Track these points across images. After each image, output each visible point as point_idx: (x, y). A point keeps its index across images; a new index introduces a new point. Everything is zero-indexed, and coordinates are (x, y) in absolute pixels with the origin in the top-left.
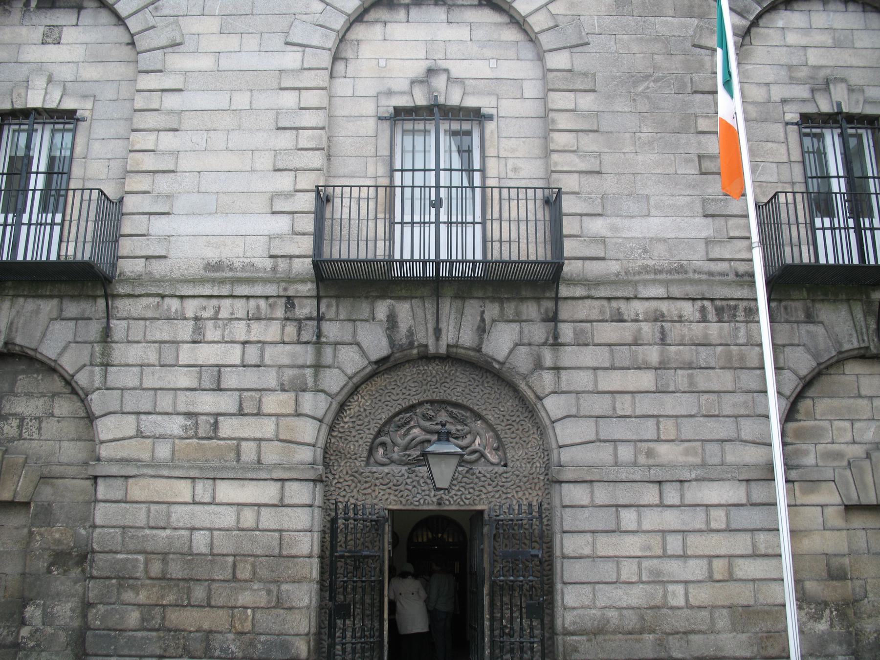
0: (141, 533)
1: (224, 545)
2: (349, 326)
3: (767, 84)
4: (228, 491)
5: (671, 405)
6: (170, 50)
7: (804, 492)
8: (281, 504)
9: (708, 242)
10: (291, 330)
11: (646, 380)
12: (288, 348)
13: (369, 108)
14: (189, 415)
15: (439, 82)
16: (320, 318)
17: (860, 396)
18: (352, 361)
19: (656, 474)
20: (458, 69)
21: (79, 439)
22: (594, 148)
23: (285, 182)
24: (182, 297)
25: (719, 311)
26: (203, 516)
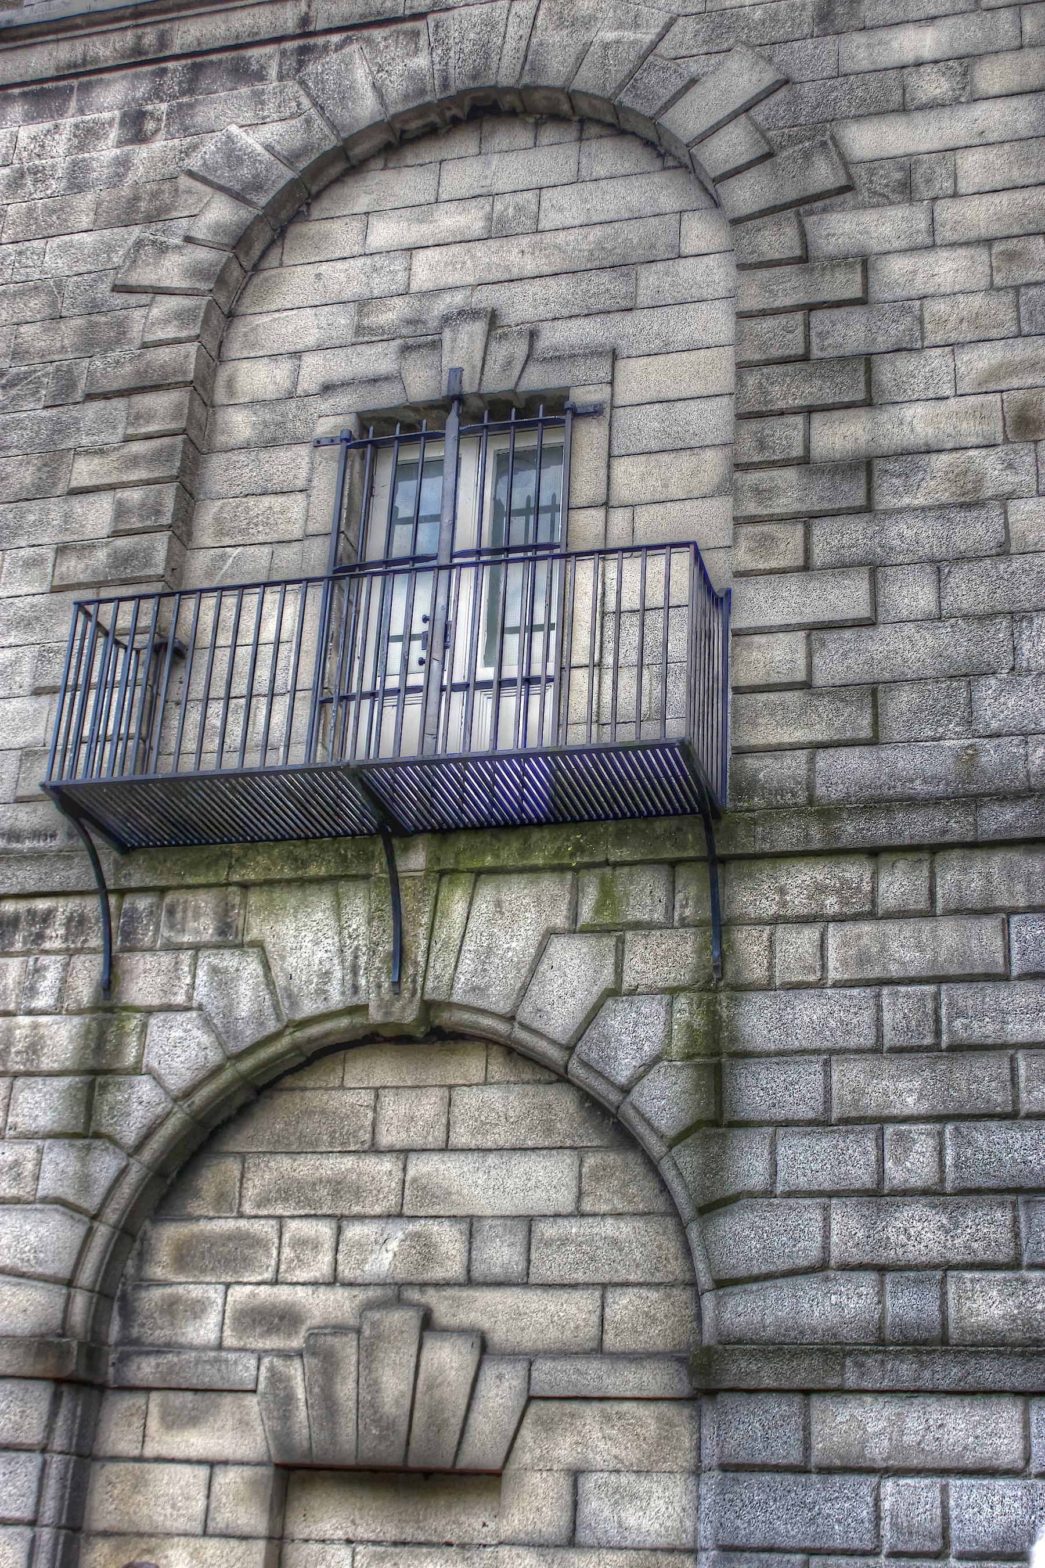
3: (296, 355)
7: (173, 1421)
17: (375, 1150)
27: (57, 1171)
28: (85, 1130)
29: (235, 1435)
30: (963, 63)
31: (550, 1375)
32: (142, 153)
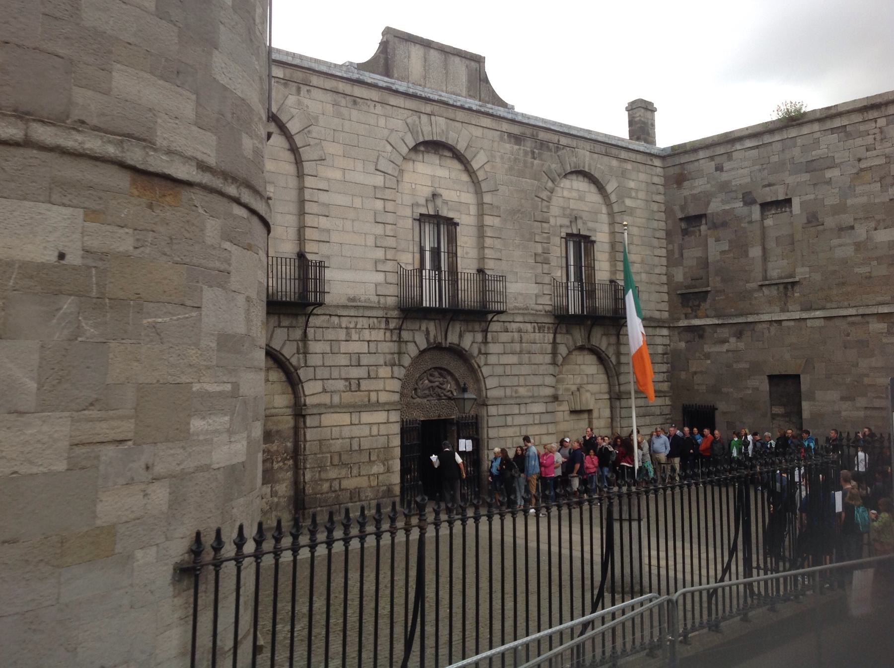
0: (328, 442)
1: (366, 444)
2: (411, 333)
4: (366, 417)
5: (525, 370)
6: (319, 162)
8: (388, 422)
9: (537, 296)
10: (388, 334)
11: (513, 359)
12: (388, 344)
13: (408, 212)
14: (346, 379)
15: (439, 202)
16: (400, 329)
18: (413, 350)
19: (518, 401)
20: (447, 195)
21: (283, 393)
22: (499, 247)
23: (380, 254)
24: (340, 316)
25: (539, 328)
26: (356, 431)
27: (551, 369)
28: (554, 363)
29: (565, 407)
30: (637, 190)
31: (598, 397)
32: (536, 162)
